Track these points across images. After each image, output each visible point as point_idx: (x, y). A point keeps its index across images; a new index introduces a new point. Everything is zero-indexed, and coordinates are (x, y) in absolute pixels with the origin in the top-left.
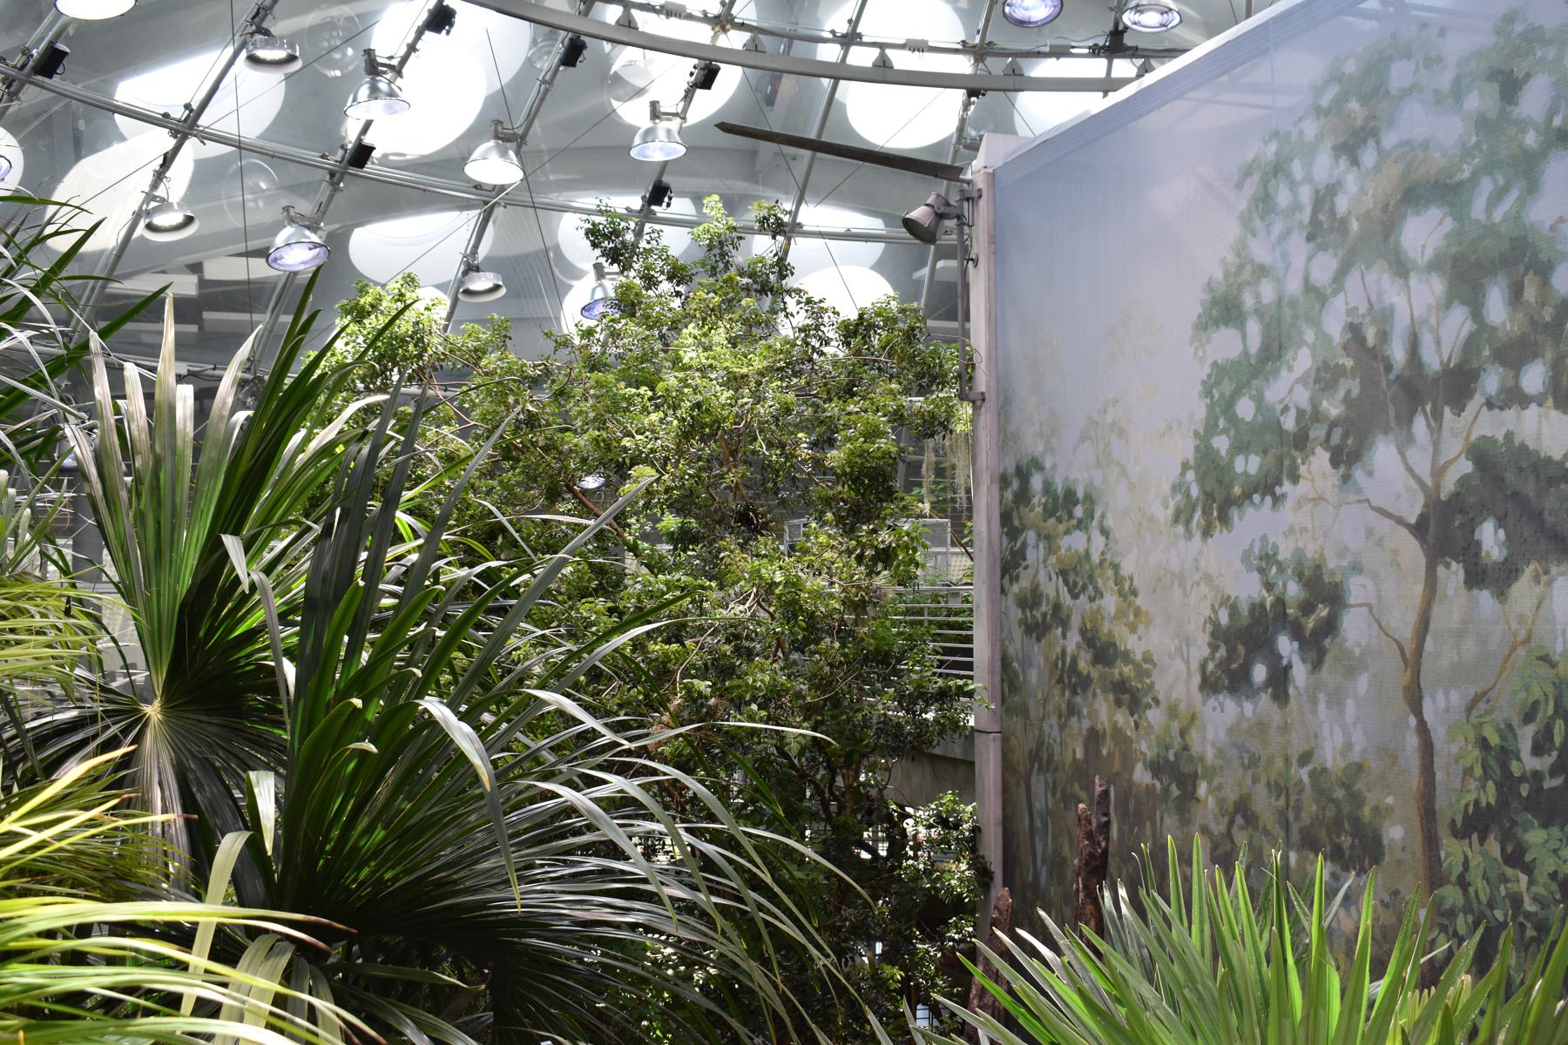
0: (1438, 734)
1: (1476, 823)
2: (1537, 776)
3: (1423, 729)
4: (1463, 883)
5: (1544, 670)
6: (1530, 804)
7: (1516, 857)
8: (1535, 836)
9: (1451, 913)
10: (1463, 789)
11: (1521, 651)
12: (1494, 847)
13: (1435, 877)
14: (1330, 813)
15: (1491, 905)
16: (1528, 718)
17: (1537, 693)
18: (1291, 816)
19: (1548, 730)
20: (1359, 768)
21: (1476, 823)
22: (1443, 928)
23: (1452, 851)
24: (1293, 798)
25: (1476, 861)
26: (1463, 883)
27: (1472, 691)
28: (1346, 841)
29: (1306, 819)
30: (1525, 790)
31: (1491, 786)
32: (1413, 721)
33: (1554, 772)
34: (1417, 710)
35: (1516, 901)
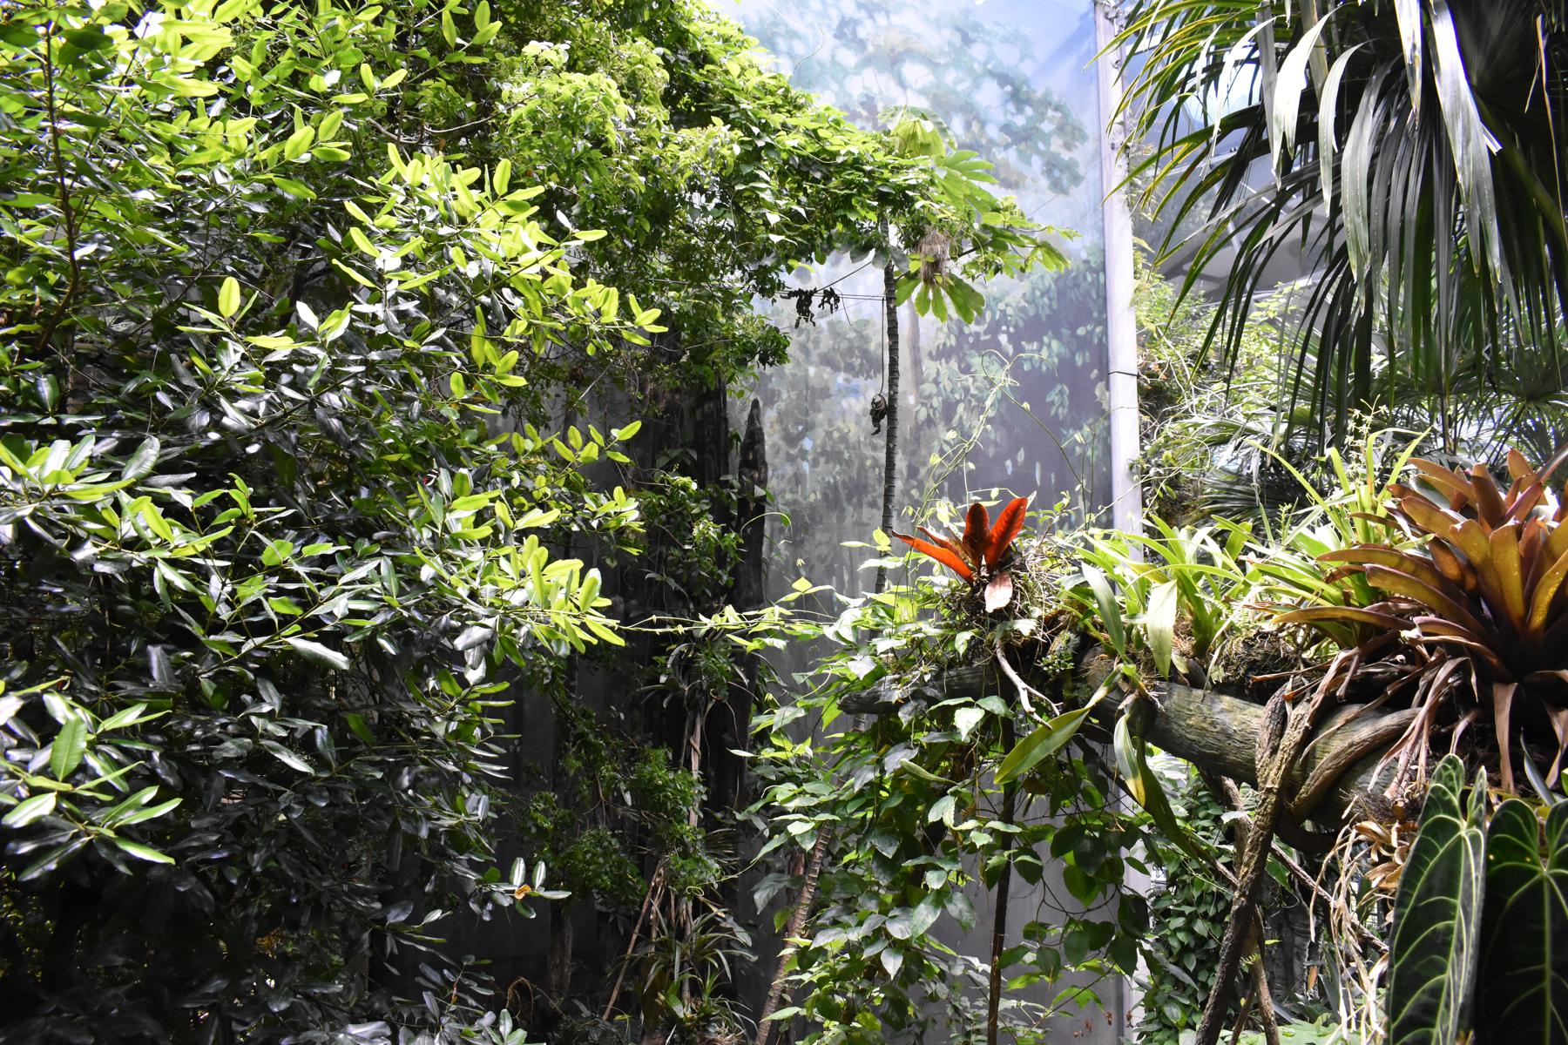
1: (943, 354)
2: (977, 334)
4: (936, 382)
6: (972, 346)
7: (966, 369)
8: (976, 361)
9: (930, 397)
10: (937, 337)
12: (954, 364)
14: (844, 345)
15: (952, 392)
18: (810, 345)
20: (866, 323)
21: (943, 354)
22: (924, 404)
23: (929, 367)
24: (812, 337)
25: (944, 371)
26: (936, 382)
28: (857, 362)
29: (823, 348)
30: (971, 340)
31: (953, 338)
33: (986, 333)
35: (967, 390)
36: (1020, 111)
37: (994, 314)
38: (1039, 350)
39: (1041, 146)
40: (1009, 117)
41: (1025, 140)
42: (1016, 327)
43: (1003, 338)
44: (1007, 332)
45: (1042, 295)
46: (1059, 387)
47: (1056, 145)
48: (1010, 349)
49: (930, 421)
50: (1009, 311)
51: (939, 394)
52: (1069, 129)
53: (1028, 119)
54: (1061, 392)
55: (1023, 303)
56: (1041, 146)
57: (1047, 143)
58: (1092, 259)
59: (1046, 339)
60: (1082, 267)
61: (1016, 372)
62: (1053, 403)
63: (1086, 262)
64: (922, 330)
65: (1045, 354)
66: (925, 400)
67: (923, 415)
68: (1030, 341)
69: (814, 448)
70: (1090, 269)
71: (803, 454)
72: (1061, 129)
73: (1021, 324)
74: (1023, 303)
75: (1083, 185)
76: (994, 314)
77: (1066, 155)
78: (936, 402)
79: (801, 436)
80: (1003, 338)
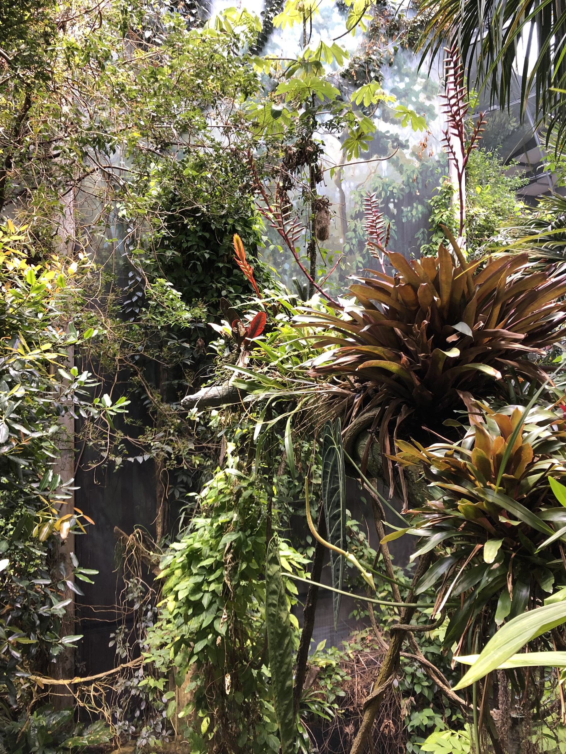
0: (347, 194)
3: (342, 192)
4: (354, 231)
5: (379, 180)
9: (351, 239)
11: (373, 175)
13: (345, 229)
15: (363, 235)
16: (375, 191)
17: (377, 185)
19: (380, 194)
23: (351, 224)
25: (359, 225)
26: (354, 231)
27: (358, 183)
32: (338, 189)
33: (382, 203)
34: (340, 186)
36: (402, 80)
37: (386, 193)
38: (411, 211)
39: (414, 99)
40: (396, 84)
41: (404, 96)
42: (398, 199)
43: (391, 206)
44: (394, 202)
45: (414, 180)
46: (422, 230)
47: (422, 97)
48: (395, 212)
49: (351, 252)
50: (395, 191)
51: (356, 237)
52: (429, 88)
53: (406, 84)
54: (423, 232)
55: (402, 186)
56: (414, 99)
57: (417, 97)
58: (441, 160)
59: (415, 205)
60: (436, 164)
61: (398, 223)
62: (418, 238)
63: (439, 161)
64: (347, 204)
65: (414, 212)
66: (348, 240)
67: (347, 248)
68: (406, 207)
69: (290, 268)
70: (441, 166)
71: (284, 271)
72: (425, 88)
73: (401, 197)
74: (402, 186)
75: (437, 119)
76: (386, 193)
77: (427, 103)
78: (354, 241)
79: (283, 262)
80: (391, 206)
